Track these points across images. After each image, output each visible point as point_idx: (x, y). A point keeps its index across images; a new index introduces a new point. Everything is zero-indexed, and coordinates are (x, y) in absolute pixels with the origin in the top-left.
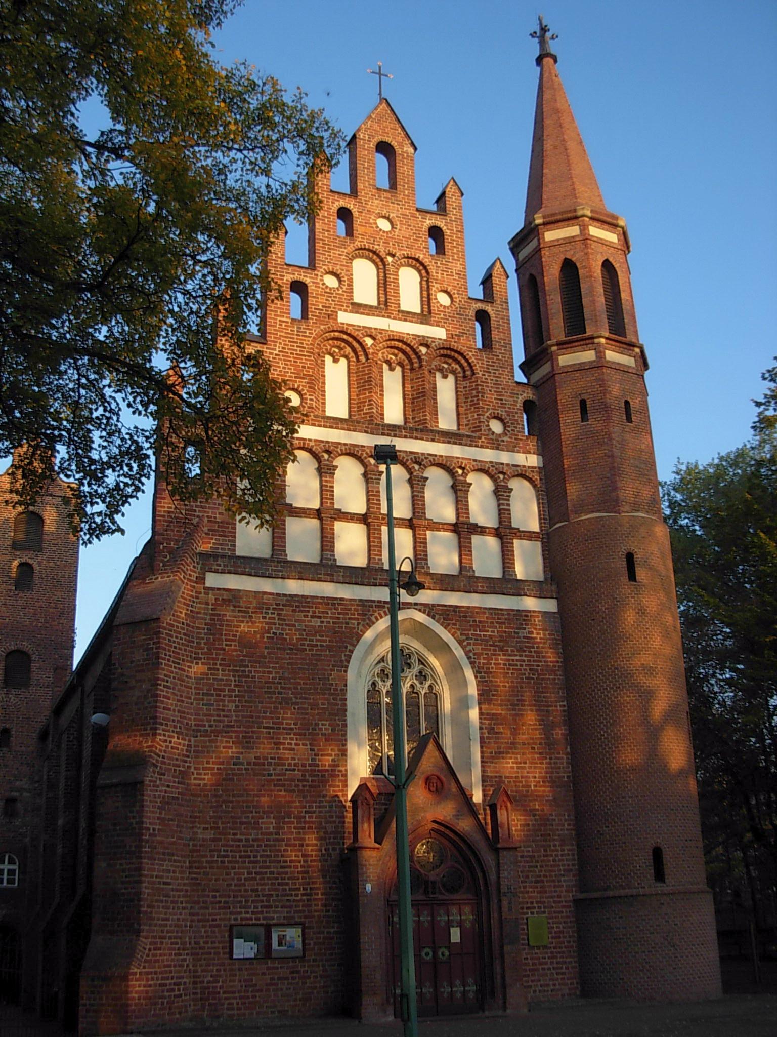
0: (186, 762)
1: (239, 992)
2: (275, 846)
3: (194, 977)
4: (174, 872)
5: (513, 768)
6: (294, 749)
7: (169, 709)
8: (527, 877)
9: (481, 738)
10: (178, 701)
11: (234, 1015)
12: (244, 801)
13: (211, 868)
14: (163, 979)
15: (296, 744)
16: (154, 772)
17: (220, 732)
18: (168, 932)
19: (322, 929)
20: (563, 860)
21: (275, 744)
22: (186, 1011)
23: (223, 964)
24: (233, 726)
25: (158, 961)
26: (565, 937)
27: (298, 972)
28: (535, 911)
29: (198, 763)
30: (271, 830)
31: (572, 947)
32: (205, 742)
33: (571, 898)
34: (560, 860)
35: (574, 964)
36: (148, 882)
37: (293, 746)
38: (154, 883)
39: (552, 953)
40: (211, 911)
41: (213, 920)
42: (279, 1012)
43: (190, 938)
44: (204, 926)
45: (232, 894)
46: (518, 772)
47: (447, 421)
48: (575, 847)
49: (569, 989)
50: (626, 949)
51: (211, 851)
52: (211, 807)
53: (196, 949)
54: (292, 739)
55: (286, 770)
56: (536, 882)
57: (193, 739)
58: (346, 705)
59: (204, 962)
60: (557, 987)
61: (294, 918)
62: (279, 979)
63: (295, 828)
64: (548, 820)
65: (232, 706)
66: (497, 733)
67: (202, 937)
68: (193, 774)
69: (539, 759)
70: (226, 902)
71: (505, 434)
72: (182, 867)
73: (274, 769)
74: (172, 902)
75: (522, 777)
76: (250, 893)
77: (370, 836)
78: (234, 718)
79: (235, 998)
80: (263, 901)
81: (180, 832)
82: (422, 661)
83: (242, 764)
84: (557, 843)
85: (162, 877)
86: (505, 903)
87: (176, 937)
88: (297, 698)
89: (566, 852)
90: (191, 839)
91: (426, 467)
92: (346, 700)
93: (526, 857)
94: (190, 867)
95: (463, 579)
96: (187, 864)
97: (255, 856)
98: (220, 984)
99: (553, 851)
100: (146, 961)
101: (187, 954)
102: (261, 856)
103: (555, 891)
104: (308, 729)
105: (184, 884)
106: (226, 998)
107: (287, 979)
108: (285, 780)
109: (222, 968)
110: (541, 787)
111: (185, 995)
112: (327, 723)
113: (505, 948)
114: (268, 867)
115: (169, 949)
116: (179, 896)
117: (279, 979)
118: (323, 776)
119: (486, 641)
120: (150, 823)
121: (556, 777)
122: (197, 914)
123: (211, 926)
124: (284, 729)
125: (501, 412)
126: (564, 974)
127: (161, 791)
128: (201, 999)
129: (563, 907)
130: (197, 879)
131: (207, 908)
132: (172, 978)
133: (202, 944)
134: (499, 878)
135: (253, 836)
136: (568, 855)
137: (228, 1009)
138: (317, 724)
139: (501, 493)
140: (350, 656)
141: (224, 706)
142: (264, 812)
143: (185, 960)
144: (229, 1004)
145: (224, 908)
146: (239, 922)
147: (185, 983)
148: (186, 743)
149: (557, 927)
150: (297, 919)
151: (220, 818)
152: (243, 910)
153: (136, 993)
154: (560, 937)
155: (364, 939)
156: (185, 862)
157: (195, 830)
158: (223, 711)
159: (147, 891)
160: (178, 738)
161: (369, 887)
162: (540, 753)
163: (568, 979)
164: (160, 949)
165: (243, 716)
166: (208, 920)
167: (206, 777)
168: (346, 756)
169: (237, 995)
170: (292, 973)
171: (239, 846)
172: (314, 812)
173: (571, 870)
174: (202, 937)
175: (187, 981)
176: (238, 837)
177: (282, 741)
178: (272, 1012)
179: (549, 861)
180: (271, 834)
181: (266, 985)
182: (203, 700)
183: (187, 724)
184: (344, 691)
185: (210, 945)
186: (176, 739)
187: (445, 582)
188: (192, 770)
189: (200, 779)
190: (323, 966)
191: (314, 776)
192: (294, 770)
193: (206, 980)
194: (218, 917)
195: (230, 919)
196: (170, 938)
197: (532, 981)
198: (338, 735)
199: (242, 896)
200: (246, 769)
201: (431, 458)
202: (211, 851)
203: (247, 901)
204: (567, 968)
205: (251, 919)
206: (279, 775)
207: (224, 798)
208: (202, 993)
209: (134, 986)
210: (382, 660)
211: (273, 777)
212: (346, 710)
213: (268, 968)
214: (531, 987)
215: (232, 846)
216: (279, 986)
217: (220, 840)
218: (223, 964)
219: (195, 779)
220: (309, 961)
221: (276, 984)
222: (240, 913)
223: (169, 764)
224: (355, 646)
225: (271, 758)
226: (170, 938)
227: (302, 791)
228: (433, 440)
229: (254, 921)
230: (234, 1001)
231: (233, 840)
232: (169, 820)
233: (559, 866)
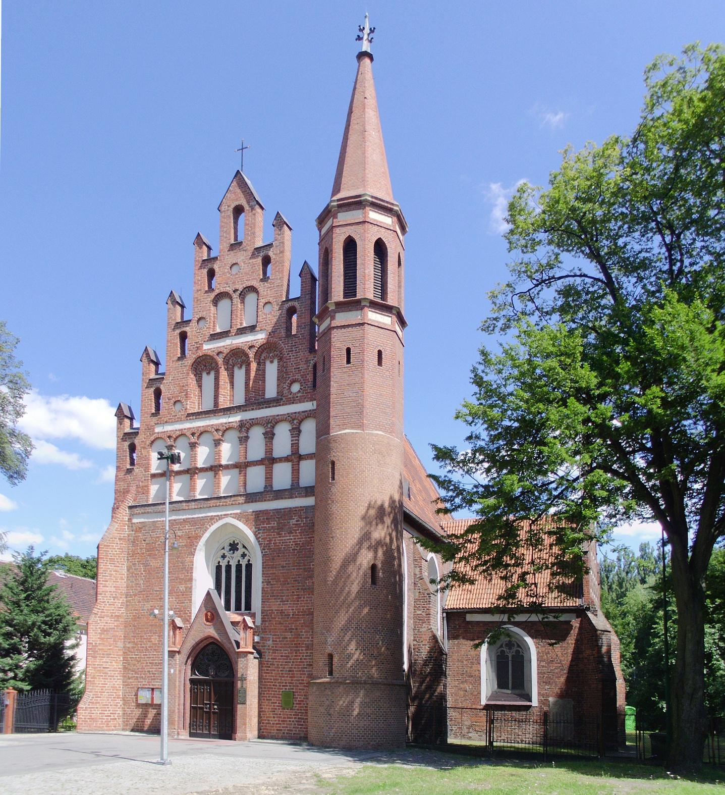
8: (284, 668)
47: (271, 391)
56: (290, 671)
58: (192, 576)
71: (299, 391)
82: (244, 547)
91: (248, 429)
95: (270, 492)
119: (270, 530)
125: (298, 377)
129: (305, 686)
139: (296, 432)
140: (195, 549)
184: (192, 569)
187: (251, 498)
201: (250, 422)
210: (223, 548)
224: (198, 543)
228: (253, 409)
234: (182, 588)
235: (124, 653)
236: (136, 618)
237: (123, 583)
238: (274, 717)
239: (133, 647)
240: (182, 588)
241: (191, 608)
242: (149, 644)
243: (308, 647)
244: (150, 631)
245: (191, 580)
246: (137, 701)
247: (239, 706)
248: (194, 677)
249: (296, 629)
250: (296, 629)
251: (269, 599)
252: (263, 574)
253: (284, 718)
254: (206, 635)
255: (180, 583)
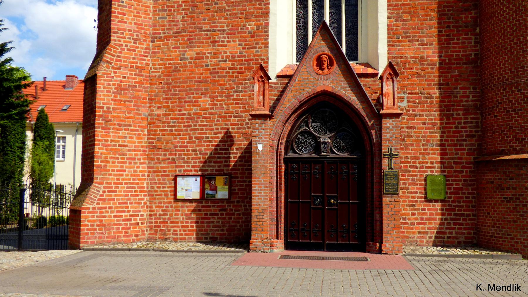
0: (144, 60)
1: (182, 222)
2: (210, 118)
3: (151, 211)
4: (130, 138)
5: (419, 49)
6: (225, 46)
7: (125, 22)
8: (428, 141)
9: (389, 26)
10: (135, 16)
11: (177, 238)
12: (188, 86)
13: (164, 135)
14: (117, 212)
15: (228, 42)
16: (108, 67)
17: (170, 37)
18: (123, 179)
19: (245, 179)
20: (465, 127)
21: (212, 42)
22: (144, 234)
23: (170, 203)
24: (180, 32)
25: (113, 200)
26: (464, 193)
27: (226, 210)
28: (435, 169)
29: (155, 60)
30: (208, 106)
31: (471, 202)
32: (160, 45)
33: (472, 160)
34: (462, 127)
35: (472, 217)
36: (103, 145)
37: (226, 43)
38: (109, 145)
39: (449, 206)
40: (162, 165)
41: (164, 171)
42: (211, 238)
43: (147, 184)
44: (157, 176)
45: (178, 153)
46: (423, 53)
48: (479, 116)
49: (466, 238)
50: (514, 208)
51: (163, 122)
52: (164, 92)
53: (152, 191)
54: (224, 38)
55: (220, 61)
57: (151, 44)
58: (268, 8)
59: (157, 201)
60: (454, 235)
61: (223, 170)
62: (211, 214)
63: (226, 104)
64: (452, 93)
65: (180, 18)
66: (404, 20)
67: (156, 183)
68: (151, 68)
69: (445, 40)
70: (173, 159)
72: (139, 134)
73: (211, 61)
74: (128, 159)
75: (427, 57)
76: (191, 152)
77: (264, 106)
78: (181, 26)
79: (178, 227)
80: (200, 158)
81: (138, 110)
83: (187, 59)
84: (461, 113)
85: (118, 141)
86: (385, 162)
87: (131, 183)
88: (229, 7)
89: (469, 120)
90: (149, 115)
92: (269, 4)
93: (428, 124)
94: (149, 135)
96: (146, 132)
97: (196, 126)
98: (168, 216)
99: (456, 119)
100: (99, 200)
101: (145, 195)
102: (200, 125)
103: (456, 154)
104: (238, 29)
105: (142, 147)
106: (172, 227)
107: (217, 214)
108: (219, 69)
109: (169, 205)
110: (446, 64)
111: (142, 223)
112: (253, 23)
113: (384, 199)
114: (205, 133)
115: (124, 191)
116: (136, 155)
117: (211, 214)
118: (249, 64)
120: (103, 104)
121: (463, 55)
122: (153, 168)
123: (162, 176)
124: (219, 30)
126: (461, 224)
127: (115, 81)
128: (155, 227)
129: (463, 167)
130: (153, 143)
131: (160, 163)
132: (128, 211)
133: (156, 189)
134: (381, 140)
135: (194, 112)
136: (472, 123)
137: (173, 234)
138: (246, 25)
141: (174, 18)
142: (202, 94)
143: (143, 199)
144: (174, 231)
145: (172, 163)
146: (182, 173)
147: (142, 215)
148: (144, 46)
149: (457, 185)
150: (225, 172)
151: (170, 99)
152: (185, 165)
153: (89, 221)
154: (458, 193)
155: (255, 188)
156: (143, 131)
157: (152, 108)
158: (173, 21)
159: (100, 151)
160: (135, 43)
161: (260, 147)
162: (448, 35)
163: (465, 229)
164: (115, 191)
165: (188, 24)
166: (160, 172)
167: (160, 70)
168: (267, 47)
169: (180, 224)
170: (220, 210)
171: (183, 119)
172: (241, 92)
173: (474, 136)
174: (156, 183)
175: (145, 214)
176: (183, 112)
177: (217, 40)
178: (206, 238)
179: (452, 128)
180: (207, 109)
181: (202, 218)
182: (158, 15)
183: (145, 33)
185: (161, 189)
186: (132, 44)
188: (150, 66)
189: (156, 72)
190: (245, 206)
191: (241, 64)
192: (226, 61)
193: (158, 213)
194: (167, 170)
195: (175, 171)
196: (125, 184)
197: (428, 228)
198: (262, 32)
199: (185, 155)
200: (190, 63)
202: (163, 122)
203: (188, 158)
204: (464, 220)
205: (191, 171)
206: (214, 65)
207: (173, 84)
208: (156, 223)
209: (88, 217)
211: (210, 67)
212: (269, 12)
213: (203, 207)
214: (426, 233)
215: (178, 119)
216: (211, 220)
217: (170, 115)
218: (170, 203)
219: (153, 72)
220: (234, 202)
221: (209, 218)
222: (183, 167)
223: (126, 62)
225: (209, 53)
226: (125, 184)
227: (232, 77)
229: (193, 173)
230: (178, 229)
231: (179, 115)
232: (125, 101)
233: (461, 132)
234: (251, 26)
235: (149, 123)
236: (172, 71)
237: (148, 20)
238: (413, 214)
239: (165, 115)
240: (251, 26)
241: (267, 55)
242: (194, 110)
243: (466, 110)
244: (196, 90)
245: (266, 14)
246: (175, 195)
247: (386, 200)
248: (290, 155)
249: (447, 84)
250: (447, 84)
251: (400, 42)
252: (389, 6)
253: (431, 214)
254: (319, 89)
255: (248, 19)
